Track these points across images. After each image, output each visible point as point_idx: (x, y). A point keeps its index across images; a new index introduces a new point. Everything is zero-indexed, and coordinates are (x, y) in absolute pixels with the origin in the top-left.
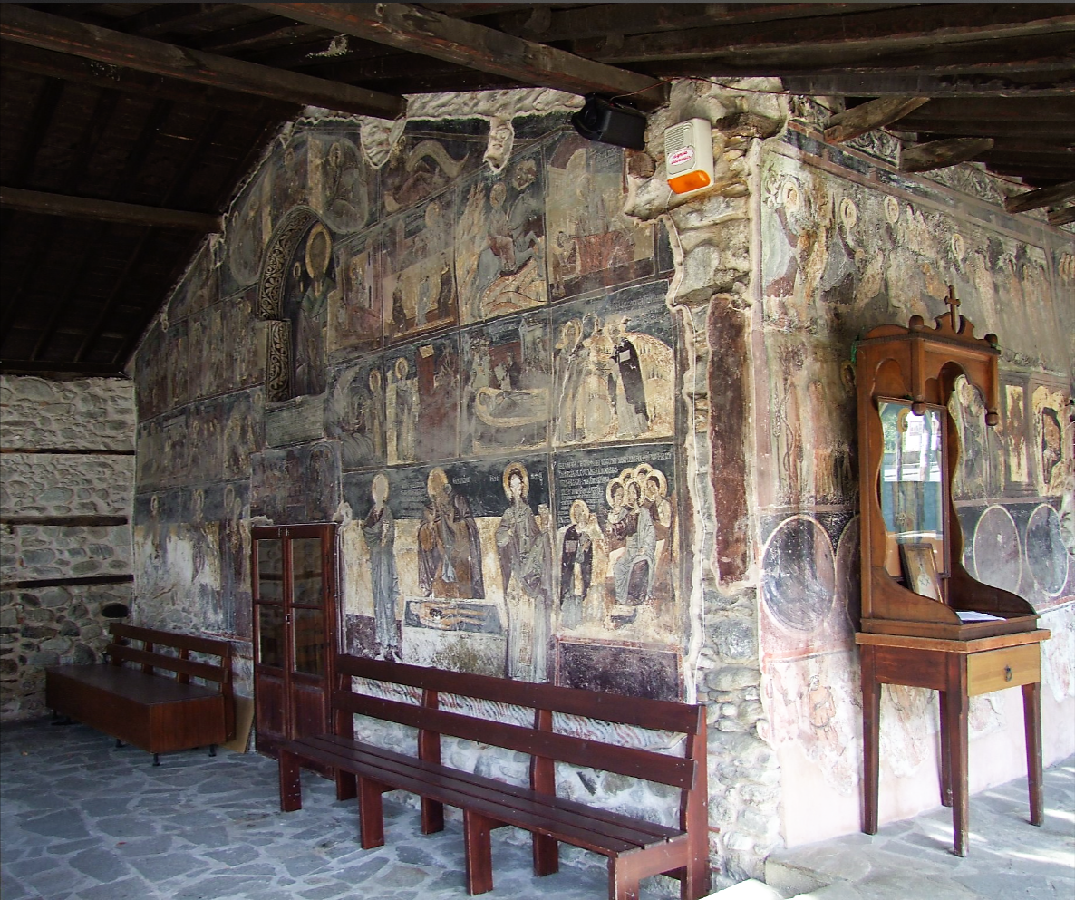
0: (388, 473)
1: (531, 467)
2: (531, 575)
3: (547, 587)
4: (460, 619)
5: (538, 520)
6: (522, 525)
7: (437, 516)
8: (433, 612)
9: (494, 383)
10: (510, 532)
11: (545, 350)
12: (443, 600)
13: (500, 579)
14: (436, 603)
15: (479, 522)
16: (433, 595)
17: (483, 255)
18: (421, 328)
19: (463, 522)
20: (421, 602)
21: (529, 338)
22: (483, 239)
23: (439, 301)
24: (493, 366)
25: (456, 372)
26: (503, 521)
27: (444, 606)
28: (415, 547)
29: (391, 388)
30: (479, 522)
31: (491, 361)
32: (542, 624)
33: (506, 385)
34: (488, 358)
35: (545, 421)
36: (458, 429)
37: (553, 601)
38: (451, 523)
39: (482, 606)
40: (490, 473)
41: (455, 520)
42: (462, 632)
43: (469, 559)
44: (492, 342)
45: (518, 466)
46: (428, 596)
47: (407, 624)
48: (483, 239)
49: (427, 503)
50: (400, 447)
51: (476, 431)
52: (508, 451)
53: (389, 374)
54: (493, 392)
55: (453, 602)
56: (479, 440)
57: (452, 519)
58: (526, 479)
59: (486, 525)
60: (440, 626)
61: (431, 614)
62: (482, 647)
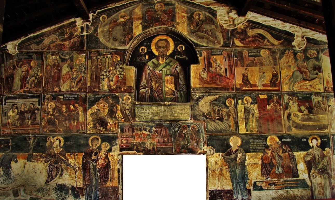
0: (240, 136)
1: (321, 137)
2: (321, 169)
3: (329, 171)
4: (286, 185)
5: (325, 152)
6: (317, 154)
7: (272, 151)
8: (270, 184)
9: (300, 111)
10: (311, 156)
11: (323, 104)
12: (276, 180)
13: (306, 171)
14: (271, 181)
15: (295, 153)
16: (270, 178)
17: (295, 72)
18: (259, 88)
19: (286, 153)
20: (263, 181)
21: (316, 100)
22: (294, 67)
23: (271, 82)
24: (299, 106)
25: (280, 105)
26: (307, 153)
27: (276, 182)
28: (260, 162)
29: (241, 107)
30: (295, 153)
31: (298, 104)
32: (327, 182)
33: (306, 112)
34: (297, 103)
35: (327, 124)
36: (283, 123)
37: (332, 176)
38: (280, 154)
39: (297, 180)
40: (302, 138)
41: (282, 153)
42: (287, 190)
43: (291, 165)
44: (299, 99)
45: (315, 136)
46: (267, 179)
47: (254, 190)
48: (294, 67)
49: (267, 147)
50: (248, 127)
51: (293, 125)
52: (310, 132)
53: (240, 101)
54: (300, 114)
55: (282, 180)
56: (295, 128)
57: (281, 153)
58: (319, 141)
59: (299, 155)
60: (274, 189)
61: (269, 185)
62: (299, 193)
